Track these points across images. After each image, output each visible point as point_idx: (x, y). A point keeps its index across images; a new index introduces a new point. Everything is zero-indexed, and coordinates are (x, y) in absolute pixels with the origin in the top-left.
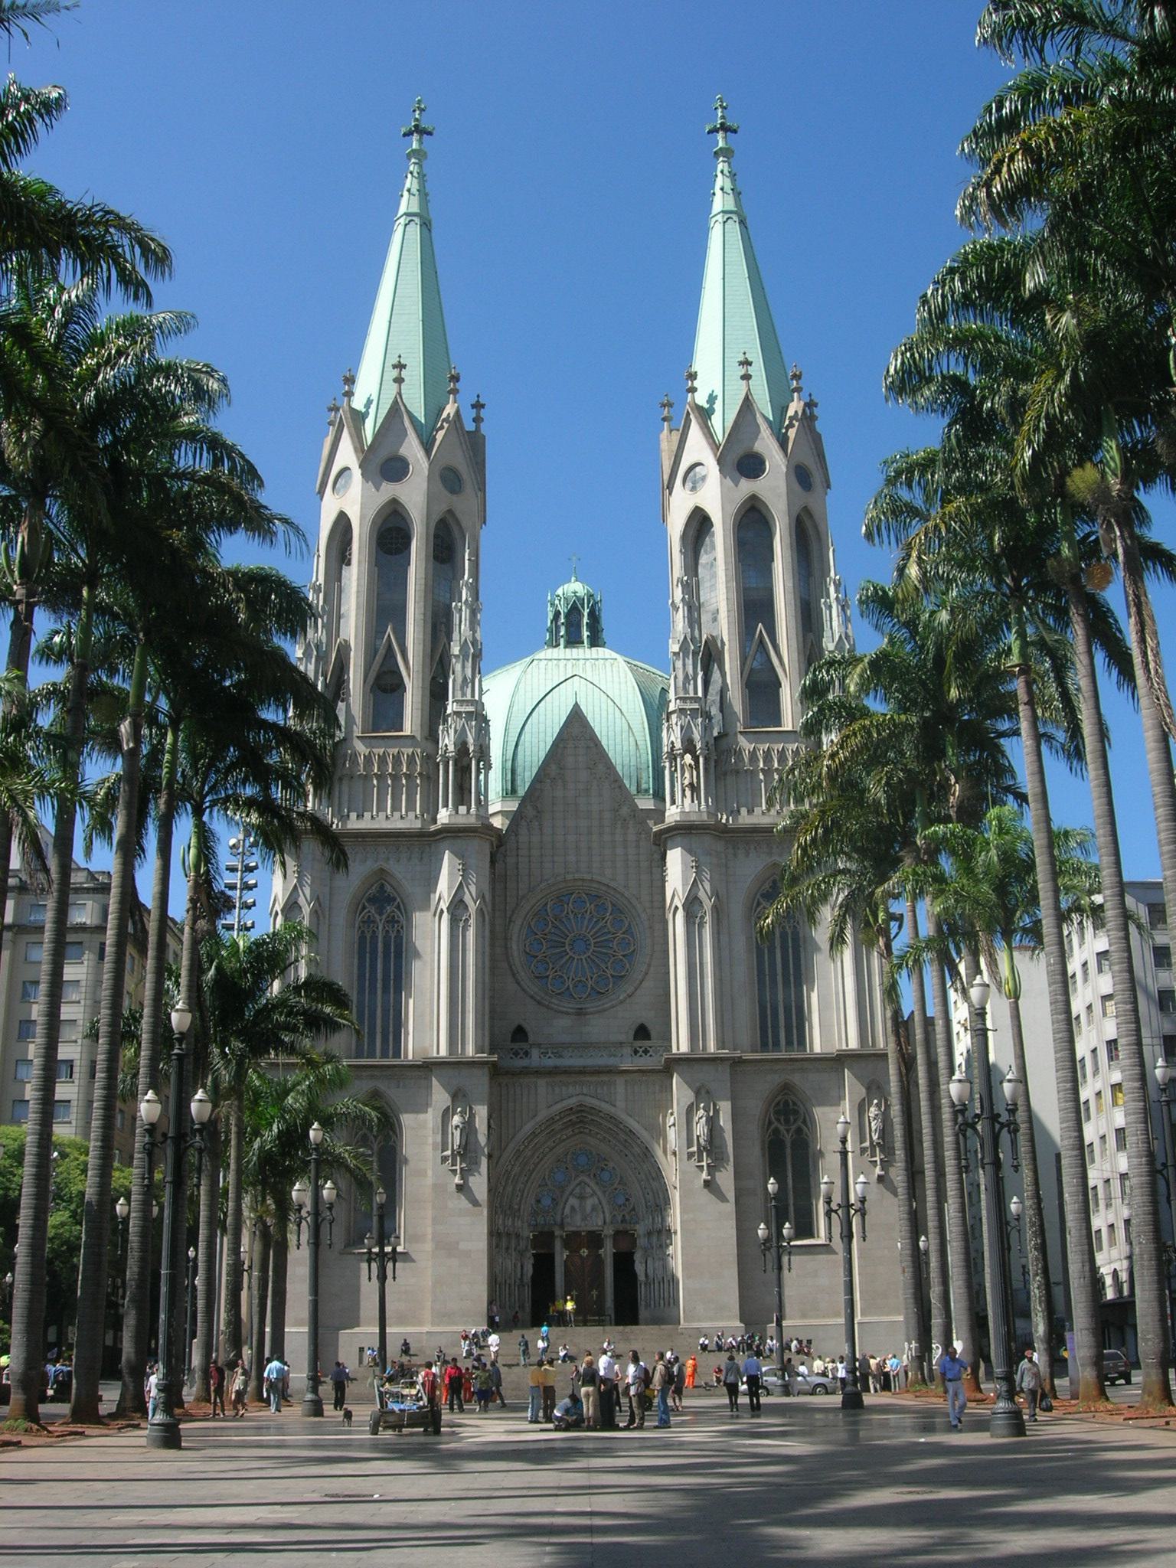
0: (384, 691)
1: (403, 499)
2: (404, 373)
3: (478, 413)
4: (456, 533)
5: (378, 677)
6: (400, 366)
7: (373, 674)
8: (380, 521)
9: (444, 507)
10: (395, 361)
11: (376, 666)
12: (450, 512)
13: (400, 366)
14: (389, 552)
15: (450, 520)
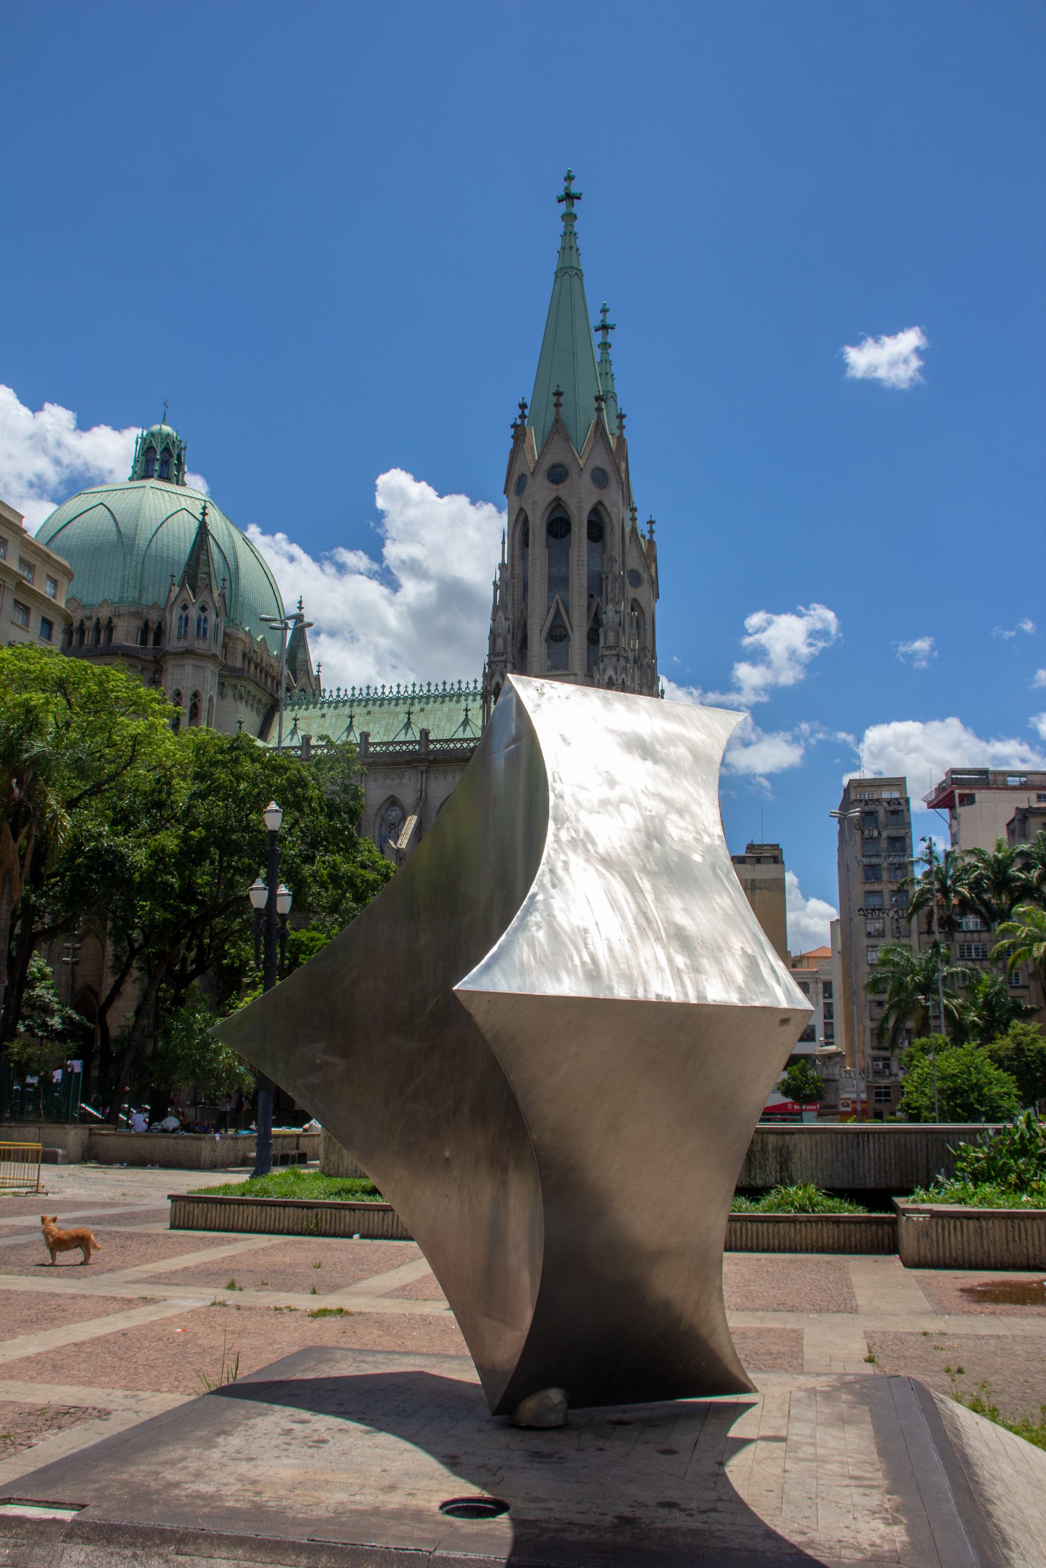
0: (555, 640)
1: (564, 497)
2: (562, 399)
3: (621, 423)
4: (606, 519)
5: (552, 629)
6: (558, 394)
7: (546, 629)
8: (548, 513)
9: (595, 500)
10: (554, 390)
11: (548, 624)
12: (600, 503)
13: (558, 394)
14: (555, 536)
15: (601, 508)
